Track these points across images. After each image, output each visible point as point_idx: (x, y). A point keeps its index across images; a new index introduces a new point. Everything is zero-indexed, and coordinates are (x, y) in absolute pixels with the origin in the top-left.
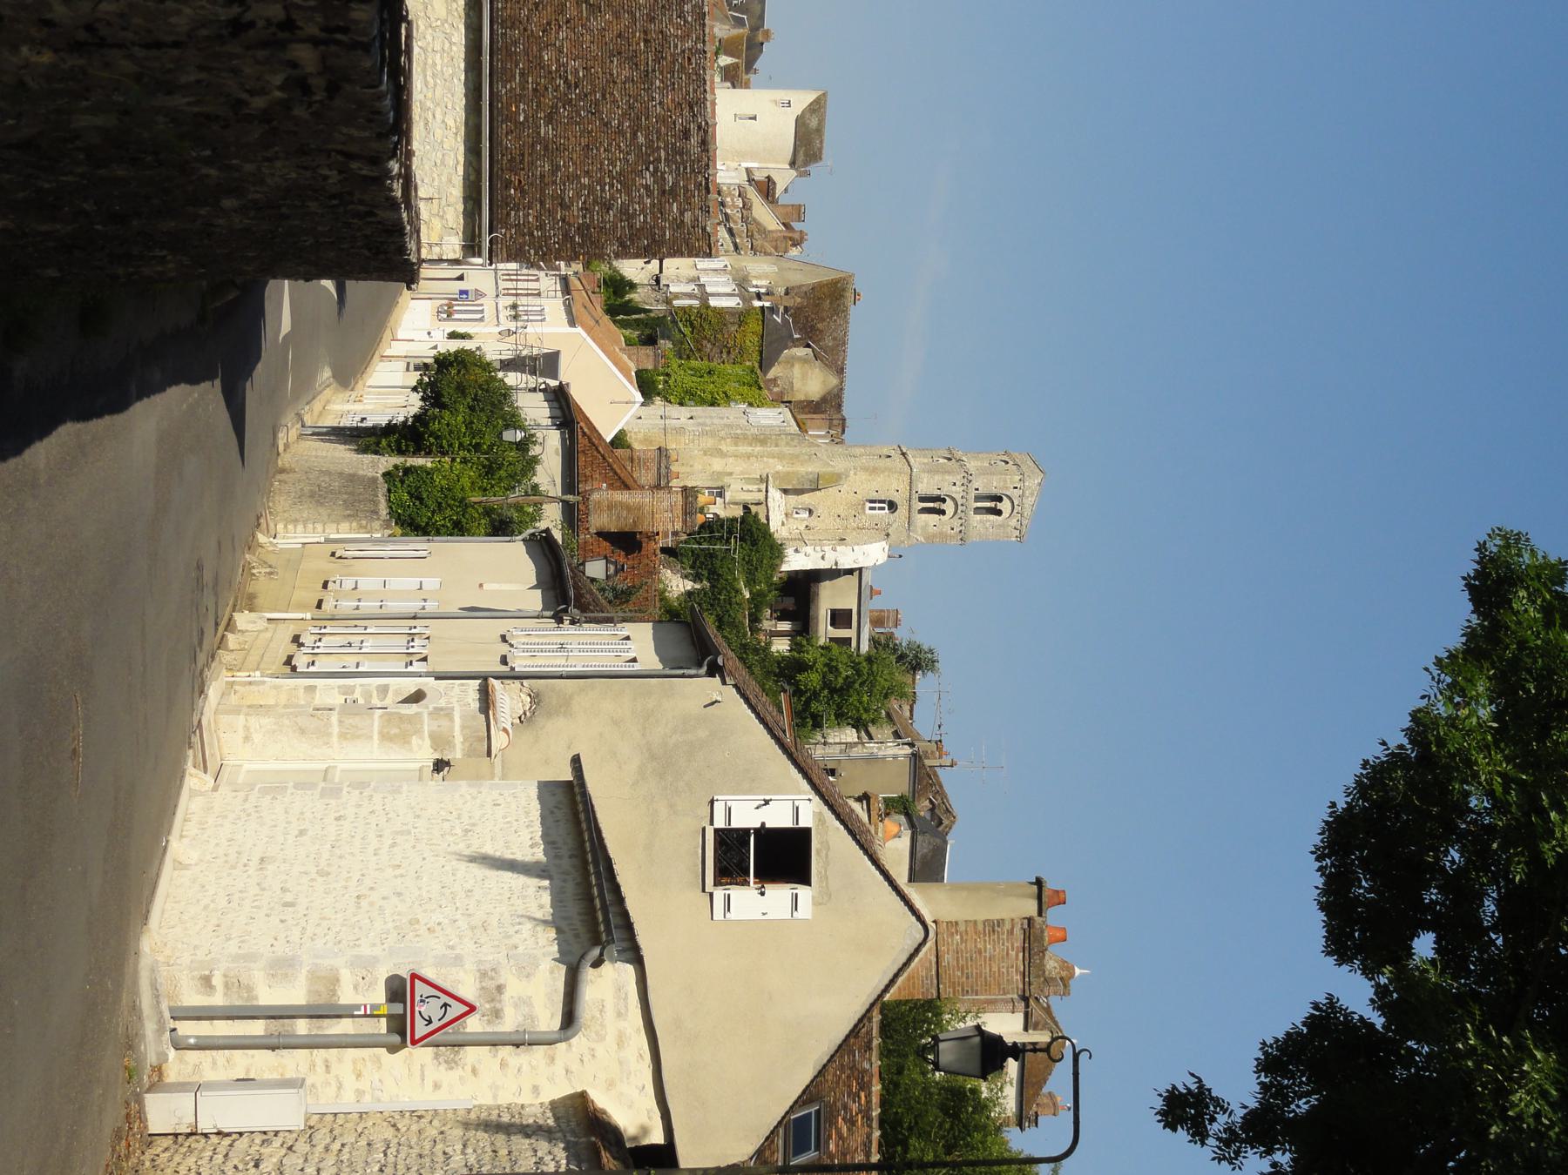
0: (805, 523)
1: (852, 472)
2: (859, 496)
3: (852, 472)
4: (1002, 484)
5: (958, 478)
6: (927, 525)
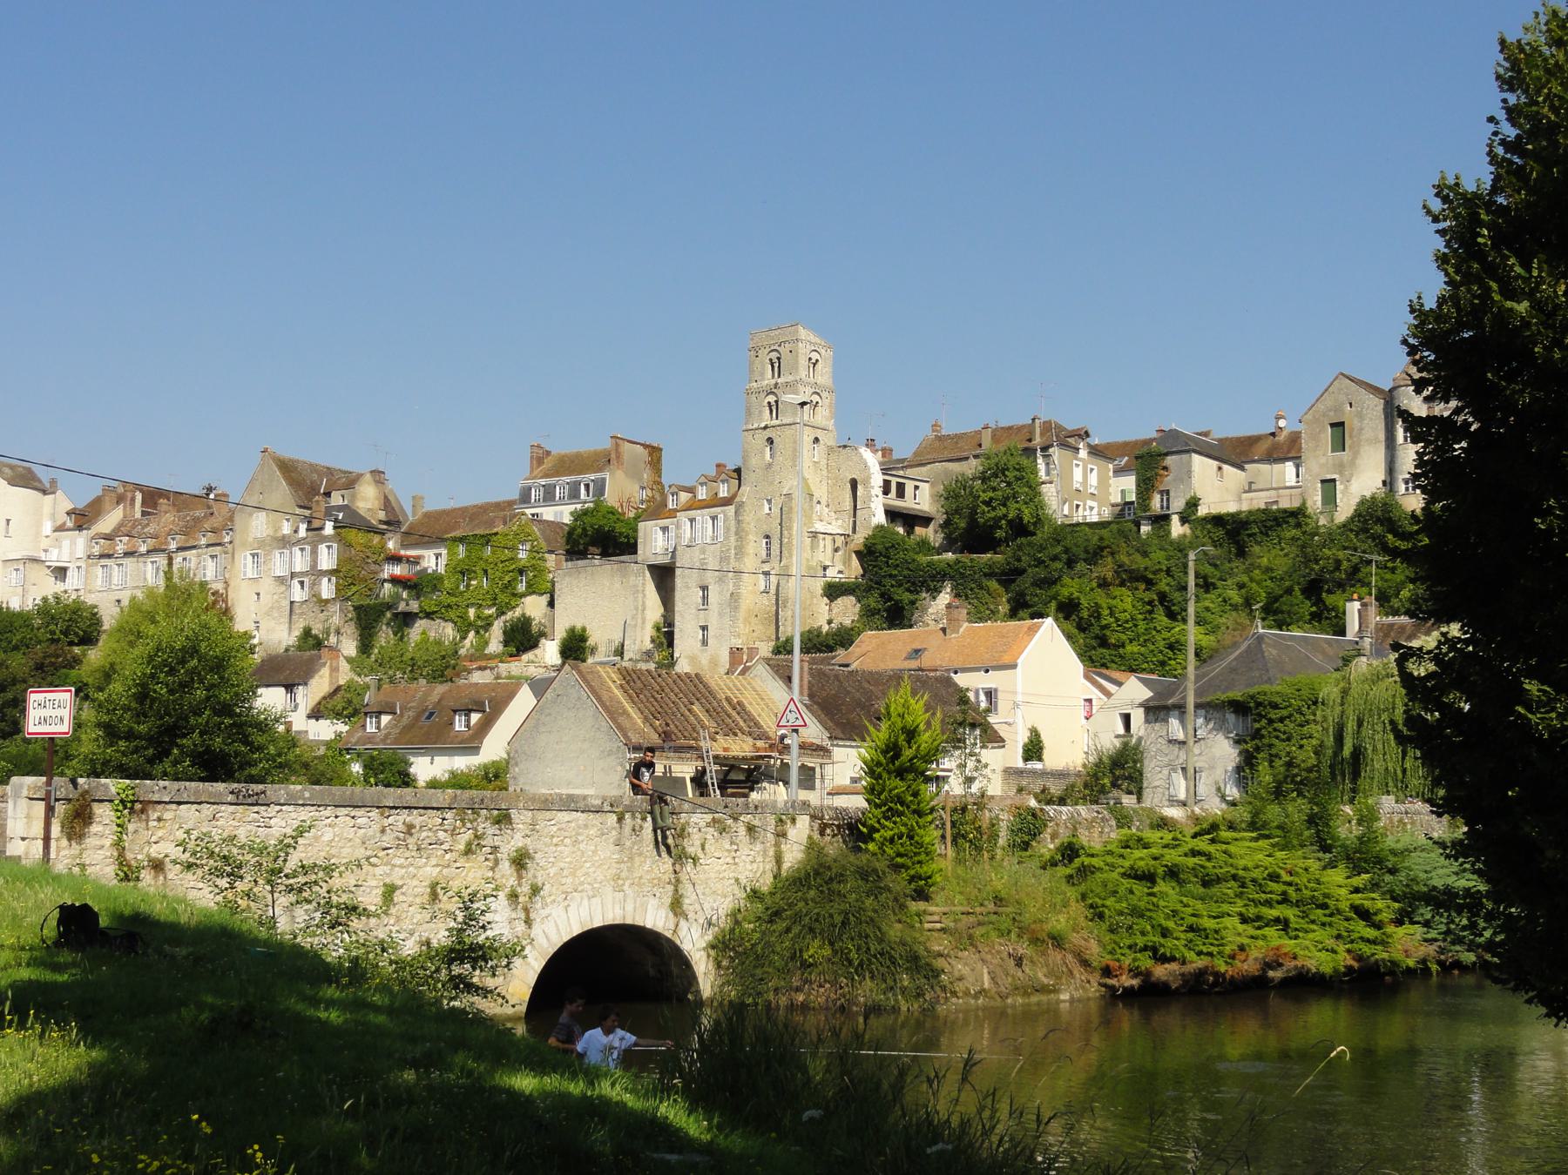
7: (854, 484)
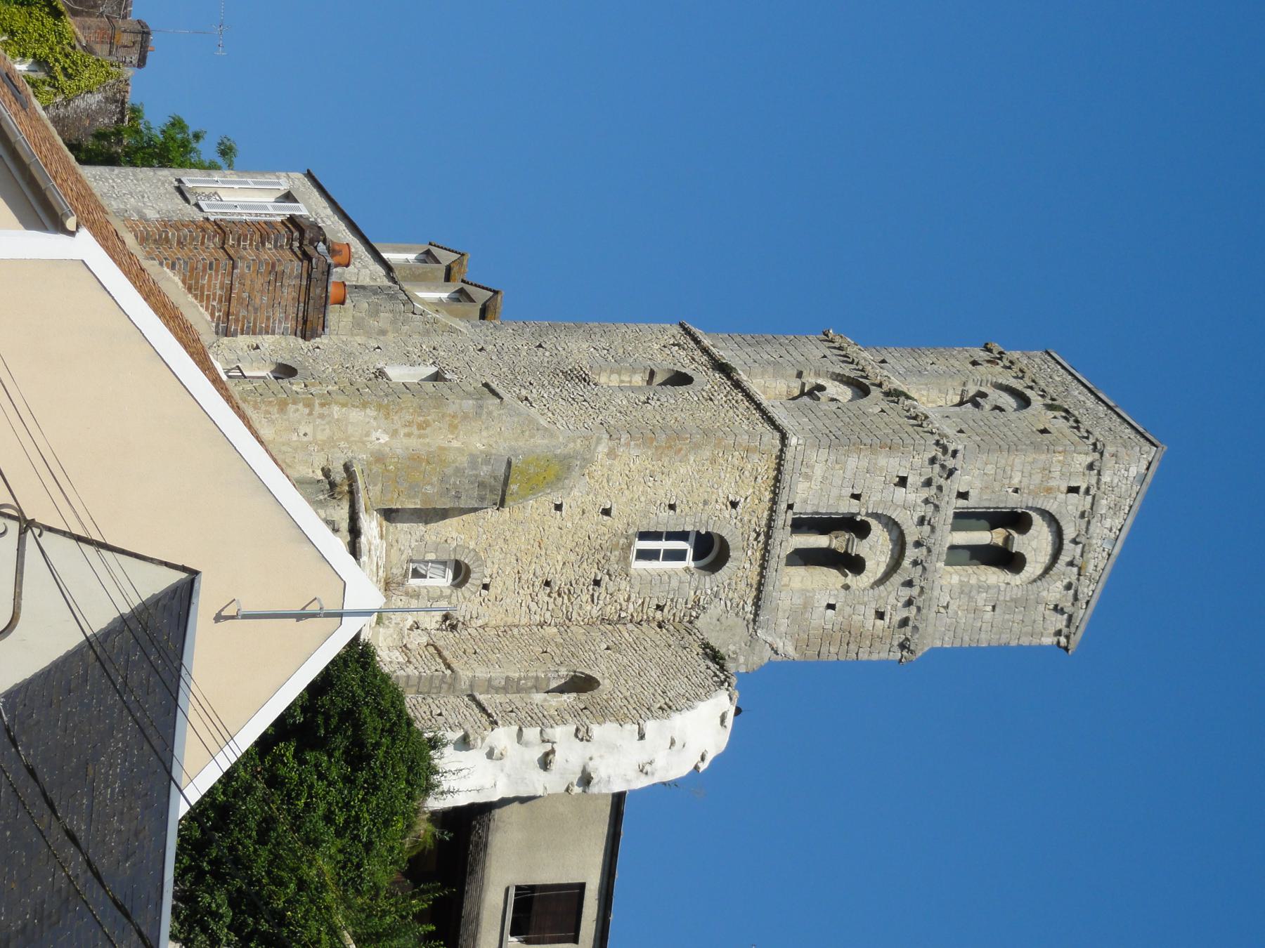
1: (602, 449)
2: (616, 523)
3: (602, 449)
4: (1037, 478)
5: (915, 465)
6: (807, 605)
7: (582, 684)
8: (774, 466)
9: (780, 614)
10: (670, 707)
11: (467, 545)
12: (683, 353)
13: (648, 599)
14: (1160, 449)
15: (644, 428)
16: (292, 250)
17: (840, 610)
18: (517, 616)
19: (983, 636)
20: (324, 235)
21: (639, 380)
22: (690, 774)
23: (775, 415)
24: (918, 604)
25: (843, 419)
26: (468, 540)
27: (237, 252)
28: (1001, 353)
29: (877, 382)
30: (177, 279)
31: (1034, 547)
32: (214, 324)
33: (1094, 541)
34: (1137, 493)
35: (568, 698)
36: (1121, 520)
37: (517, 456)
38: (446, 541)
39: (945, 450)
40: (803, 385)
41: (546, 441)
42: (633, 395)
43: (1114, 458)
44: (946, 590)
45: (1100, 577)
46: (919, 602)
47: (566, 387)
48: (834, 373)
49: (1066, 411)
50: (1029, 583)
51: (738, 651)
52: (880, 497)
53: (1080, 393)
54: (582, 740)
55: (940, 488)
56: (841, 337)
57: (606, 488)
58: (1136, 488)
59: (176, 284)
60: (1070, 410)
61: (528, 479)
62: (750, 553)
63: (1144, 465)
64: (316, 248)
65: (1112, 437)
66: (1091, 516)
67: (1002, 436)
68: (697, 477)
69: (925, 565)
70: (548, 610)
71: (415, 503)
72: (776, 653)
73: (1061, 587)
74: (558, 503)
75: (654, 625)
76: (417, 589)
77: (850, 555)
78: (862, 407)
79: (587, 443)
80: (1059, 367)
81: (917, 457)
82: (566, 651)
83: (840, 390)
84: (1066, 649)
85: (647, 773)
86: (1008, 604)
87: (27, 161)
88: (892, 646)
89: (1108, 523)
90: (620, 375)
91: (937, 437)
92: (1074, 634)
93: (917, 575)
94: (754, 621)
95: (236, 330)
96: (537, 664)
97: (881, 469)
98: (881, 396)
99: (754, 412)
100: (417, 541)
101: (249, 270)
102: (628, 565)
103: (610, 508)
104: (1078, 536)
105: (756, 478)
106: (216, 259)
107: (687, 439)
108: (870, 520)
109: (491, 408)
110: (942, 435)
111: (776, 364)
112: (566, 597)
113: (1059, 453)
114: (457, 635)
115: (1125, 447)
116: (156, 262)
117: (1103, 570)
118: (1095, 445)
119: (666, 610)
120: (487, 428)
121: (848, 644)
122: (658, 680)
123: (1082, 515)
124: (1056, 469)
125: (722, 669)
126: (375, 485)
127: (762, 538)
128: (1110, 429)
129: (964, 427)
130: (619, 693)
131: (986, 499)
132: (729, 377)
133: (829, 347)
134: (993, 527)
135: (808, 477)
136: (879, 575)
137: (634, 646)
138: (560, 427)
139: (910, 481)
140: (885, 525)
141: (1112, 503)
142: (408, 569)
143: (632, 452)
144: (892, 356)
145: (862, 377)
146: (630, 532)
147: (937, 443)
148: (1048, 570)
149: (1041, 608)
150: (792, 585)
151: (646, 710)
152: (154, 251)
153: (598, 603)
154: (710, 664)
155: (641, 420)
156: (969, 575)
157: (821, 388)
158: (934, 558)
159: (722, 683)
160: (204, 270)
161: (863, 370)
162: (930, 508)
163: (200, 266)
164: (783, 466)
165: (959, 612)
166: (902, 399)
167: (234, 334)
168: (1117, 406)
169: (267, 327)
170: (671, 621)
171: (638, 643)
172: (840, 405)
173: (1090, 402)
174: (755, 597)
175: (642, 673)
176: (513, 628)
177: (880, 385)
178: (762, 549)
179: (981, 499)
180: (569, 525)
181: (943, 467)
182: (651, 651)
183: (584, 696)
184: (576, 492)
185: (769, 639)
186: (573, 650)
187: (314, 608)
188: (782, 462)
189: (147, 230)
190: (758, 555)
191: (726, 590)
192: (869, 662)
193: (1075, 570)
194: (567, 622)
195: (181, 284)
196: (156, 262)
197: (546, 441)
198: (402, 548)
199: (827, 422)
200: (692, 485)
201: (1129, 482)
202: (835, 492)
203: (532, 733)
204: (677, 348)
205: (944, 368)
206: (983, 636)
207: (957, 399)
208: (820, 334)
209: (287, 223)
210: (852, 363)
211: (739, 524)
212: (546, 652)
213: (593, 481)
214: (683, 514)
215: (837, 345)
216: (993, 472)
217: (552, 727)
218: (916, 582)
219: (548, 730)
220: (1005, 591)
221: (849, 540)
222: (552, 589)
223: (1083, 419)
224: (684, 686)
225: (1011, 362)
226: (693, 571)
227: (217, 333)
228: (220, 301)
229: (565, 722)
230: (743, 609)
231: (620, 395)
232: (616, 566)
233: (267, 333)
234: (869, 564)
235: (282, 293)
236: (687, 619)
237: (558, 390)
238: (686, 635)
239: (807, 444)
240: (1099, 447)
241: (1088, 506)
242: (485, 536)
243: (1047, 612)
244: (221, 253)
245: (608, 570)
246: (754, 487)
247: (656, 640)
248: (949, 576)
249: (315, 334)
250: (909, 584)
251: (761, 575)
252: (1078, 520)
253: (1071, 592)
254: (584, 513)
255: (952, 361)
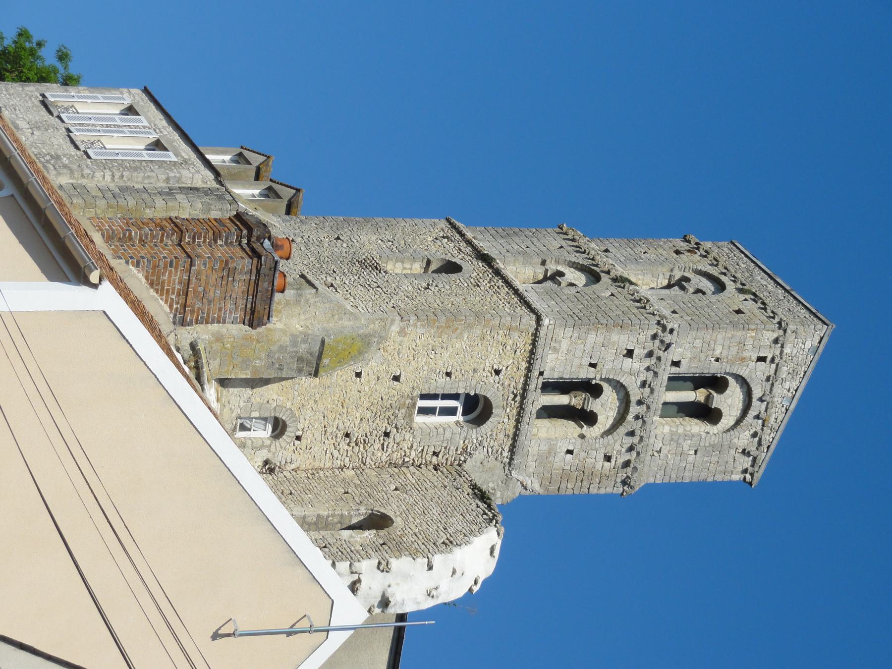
0: (263, 455)
1: (395, 328)
2: (404, 387)
3: (395, 328)
4: (734, 350)
5: (640, 341)
6: (552, 452)
8: (530, 341)
9: (530, 458)
10: (451, 542)
11: (284, 405)
12: (452, 245)
13: (426, 447)
14: (830, 327)
15: (427, 311)
16: (242, 247)
17: (577, 455)
18: (323, 461)
19: (687, 474)
20: (269, 232)
21: (418, 268)
22: (466, 595)
23: (530, 299)
24: (638, 450)
25: (583, 302)
26: (286, 401)
27: (193, 249)
28: (697, 244)
29: (606, 269)
30: (141, 276)
31: (729, 404)
32: (172, 315)
33: (776, 399)
34: (811, 362)
35: (369, 535)
36: (797, 383)
37: (329, 336)
38: (268, 402)
39: (664, 328)
40: (547, 271)
41: (351, 323)
42: (415, 281)
43: (794, 334)
44: (660, 438)
45: (779, 427)
46: (638, 448)
47: (363, 275)
48: (570, 261)
49: (754, 294)
50: (724, 432)
51: (496, 487)
52: (611, 365)
53: (761, 279)
54: (383, 571)
55: (659, 359)
56: (573, 230)
57: (397, 359)
58: (810, 358)
59: (140, 280)
60: (757, 293)
61: (337, 354)
62: (508, 410)
63: (817, 339)
64: (262, 244)
65: (791, 317)
66: (775, 380)
67: (707, 316)
68: (469, 350)
69: (645, 419)
70: (347, 456)
71: (246, 374)
72: (526, 488)
73: (749, 435)
74: (358, 371)
75: (431, 467)
76: (243, 440)
77: (586, 411)
78: (596, 292)
79: (384, 324)
80: (743, 255)
81: (641, 334)
82: (364, 492)
83: (576, 276)
84: (751, 484)
85: (433, 597)
86: (707, 448)
87: (42, 206)
88: (616, 482)
89: (787, 385)
90: (403, 264)
91: (658, 318)
92: (757, 472)
93: (638, 427)
94: (510, 464)
95: (191, 320)
96: (341, 504)
97: (614, 344)
98: (610, 282)
99: (513, 296)
100: (244, 402)
101: (205, 267)
102: (412, 420)
103: (400, 375)
104: (763, 395)
105: (516, 351)
106: (176, 258)
107: (462, 320)
108: (602, 383)
109: (308, 296)
110: (663, 317)
111: (525, 253)
112: (362, 446)
113: (752, 330)
114: (275, 477)
115: (803, 325)
116: (123, 261)
117: (781, 422)
118: (780, 323)
119: (440, 456)
120: (304, 313)
121: (582, 481)
122: (439, 517)
123: (768, 379)
124: (749, 342)
125: (489, 507)
126: (215, 360)
127: (518, 398)
128: (789, 309)
129: (677, 308)
130: (409, 530)
131: (694, 367)
132: (491, 267)
133: (564, 239)
134: (695, 388)
135: (556, 350)
136: (608, 426)
137: (417, 487)
138: (361, 310)
139: (635, 353)
140: (614, 388)
141: (791, 369)
142: (236, 424)
143: (418, 331)
144: (613, 245)
145: (593, 265)
146: (415, 394)
147: (659, 323)
148: (738, 422)
149: (732, 452)
150: (540, 434)
151: (432, 545)
152: (119, 250)
153: (387, 450)
154: (480, 503)
155: (425, 304)
156: (678, 426)
157: (561, 274)
158: (652, 413)
159: (491, 520)
160: (165, 268)
161: (593, 259)
162: (651, 374)
163: (162, 264)
164: (537, 341)
165: (669, 455)
166: (627, 285)
167: (190, 324)
168: (792, 290)
169: (219, 317)
170: (444, 465)
171: (420, 484)
172: (579, 290)
173: (771, 286)
174: (511, 445)
175: (426, 511)
176: (319, 471)
177: (608, 272)
178: (518, 407)
179: (690, 367)
180: (367, 388)
181: (662, 342)
182: (431, 491)
183: (382, 533)
184: (373, 363)
185: (521, 478)
186: (369, 490)
187: (304, 624)
188: (537, 339)
189: (112, 229)
190: (515, 412)
191: (489, 439)
192: (597, 495)
193: (760, 422)
194: (362, 465)
195: (144, 280)
196: (123, 261)
197: (351, 323)
198: (233, 408)
199: (570, 305)
200: (465, 357)
201: (805, 353)
202: (576, 362)
203: (344, 566)
204: (446, 240)
205: (655, 257)
206: (687, 474)
207: (666, 282)
208: (556, 228)
209: (235, 220)
210: (584, 252)
211: (501, 388)
212: (347, 493)
213: (386, 354)
214: (457, 380)
215: (570, 237)
216: (700, 345)
217: (359, 561)
218: (638, 432)
219: (356, 564)
220: (706, 438)
221: (585, 399)
222: (351, 439)
223: (767, 301)
224: (460, 523)
225: (706, 251)
226: (463, 424)
227: (174, 323)
228: (178, 295)
229: (369, 557)
230: (501, 454)
231: (406, 282)
232: (403, 421)
233: (219, 322)
234: (600, 418)
235: (234, 286)
236: (456, 462)
237: (356, 278)
238: (457, 476)
239: (557, 324)
240: (783, 326)
241: (772, 372)
242: (299, 398)
243: (737, 455)
244: (178, 251)
245: (396, 425)
246: (514, 359)
247: (434, 481)
248: (662, 427)
249: (261, 323)
250: (632, 434)
251: (517, 428)
252: (764, 383)
253: (756, 439)
254: (378, 379)
255: (661, 251)
